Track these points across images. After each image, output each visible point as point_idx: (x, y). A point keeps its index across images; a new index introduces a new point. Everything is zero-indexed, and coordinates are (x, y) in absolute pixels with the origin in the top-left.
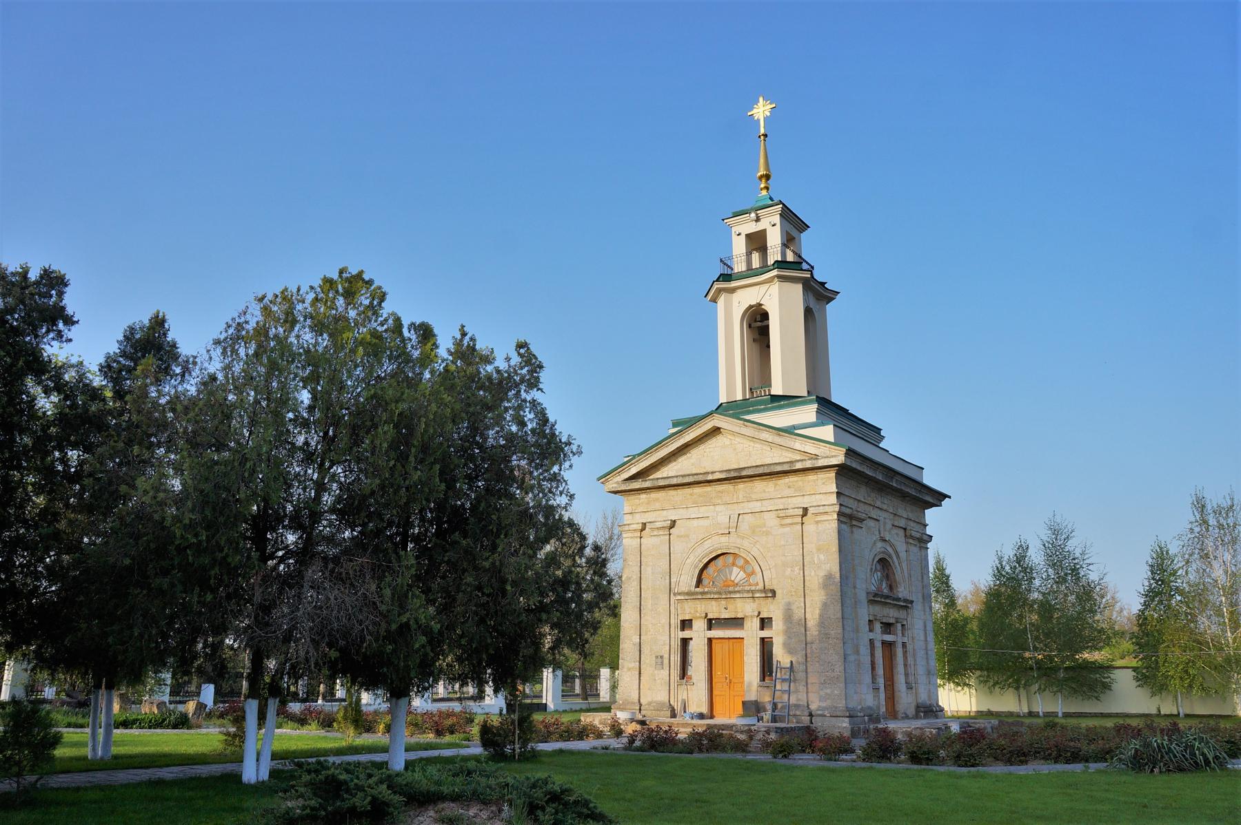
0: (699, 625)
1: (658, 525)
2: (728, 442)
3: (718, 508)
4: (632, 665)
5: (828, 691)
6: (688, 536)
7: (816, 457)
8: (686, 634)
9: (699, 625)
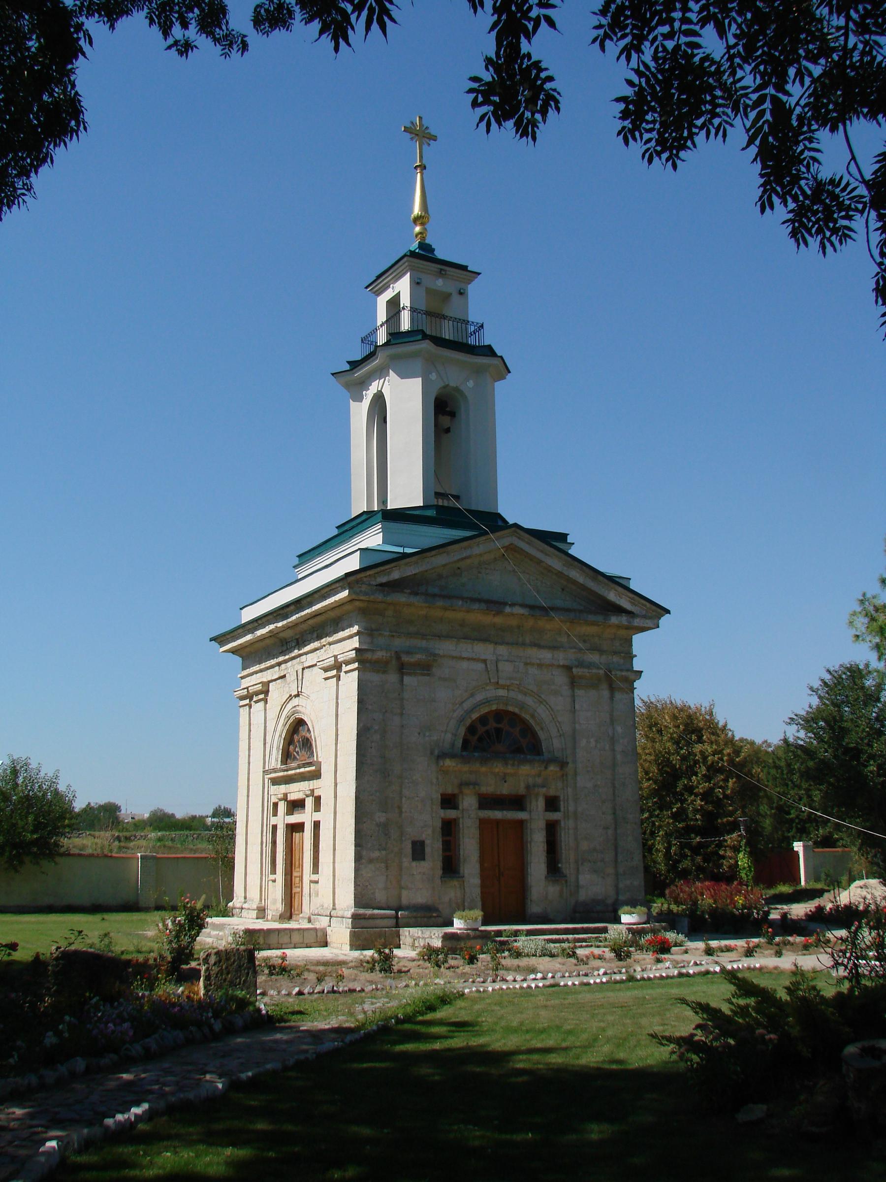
0: (469, 802)
5: (628, 882)
8: (451, 814)
9: (469, 802)
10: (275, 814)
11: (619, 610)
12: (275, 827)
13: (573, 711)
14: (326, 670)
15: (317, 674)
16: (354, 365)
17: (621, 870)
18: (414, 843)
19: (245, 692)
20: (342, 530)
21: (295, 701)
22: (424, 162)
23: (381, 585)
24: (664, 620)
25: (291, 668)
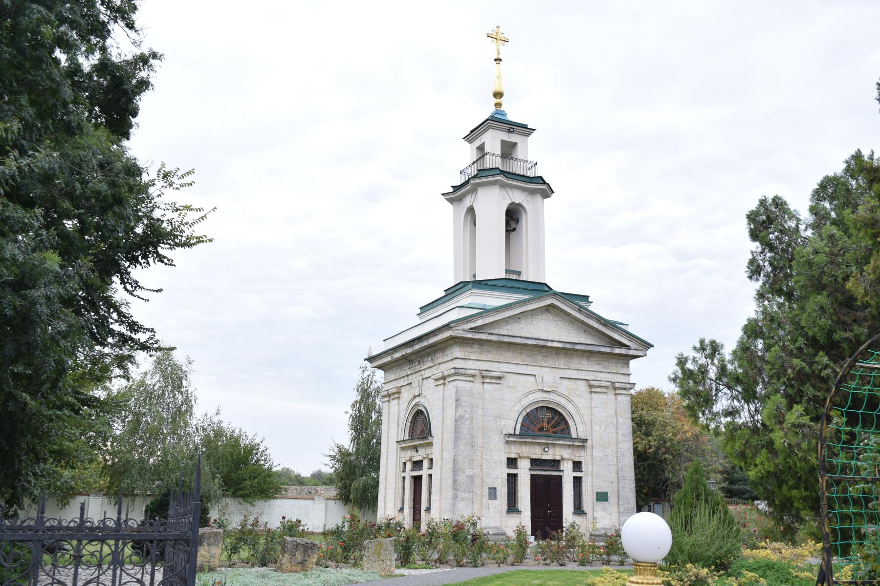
1: (494, 374)
2: (551, 318)
3: (544, 369)
4: (466, 495)
6: (516, 387)
7: (627, 347)
10: (404, 471)
11: (622, 345)
12: (404, 478)
13: (591, 408)
14: (436, 380)
15: (431, 383)
16: (456, 188)
17: (622, 510)
18: (490, 488)
19: (386, 393)
20: (448, 292)
21: (417, 400)
22: (500, 57)
23: (471, 329)
24: (650, 352)
25: (415, 379)
